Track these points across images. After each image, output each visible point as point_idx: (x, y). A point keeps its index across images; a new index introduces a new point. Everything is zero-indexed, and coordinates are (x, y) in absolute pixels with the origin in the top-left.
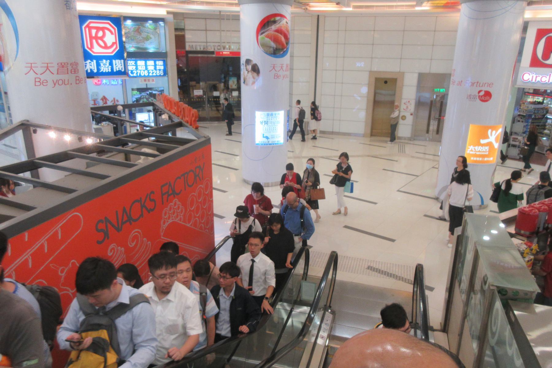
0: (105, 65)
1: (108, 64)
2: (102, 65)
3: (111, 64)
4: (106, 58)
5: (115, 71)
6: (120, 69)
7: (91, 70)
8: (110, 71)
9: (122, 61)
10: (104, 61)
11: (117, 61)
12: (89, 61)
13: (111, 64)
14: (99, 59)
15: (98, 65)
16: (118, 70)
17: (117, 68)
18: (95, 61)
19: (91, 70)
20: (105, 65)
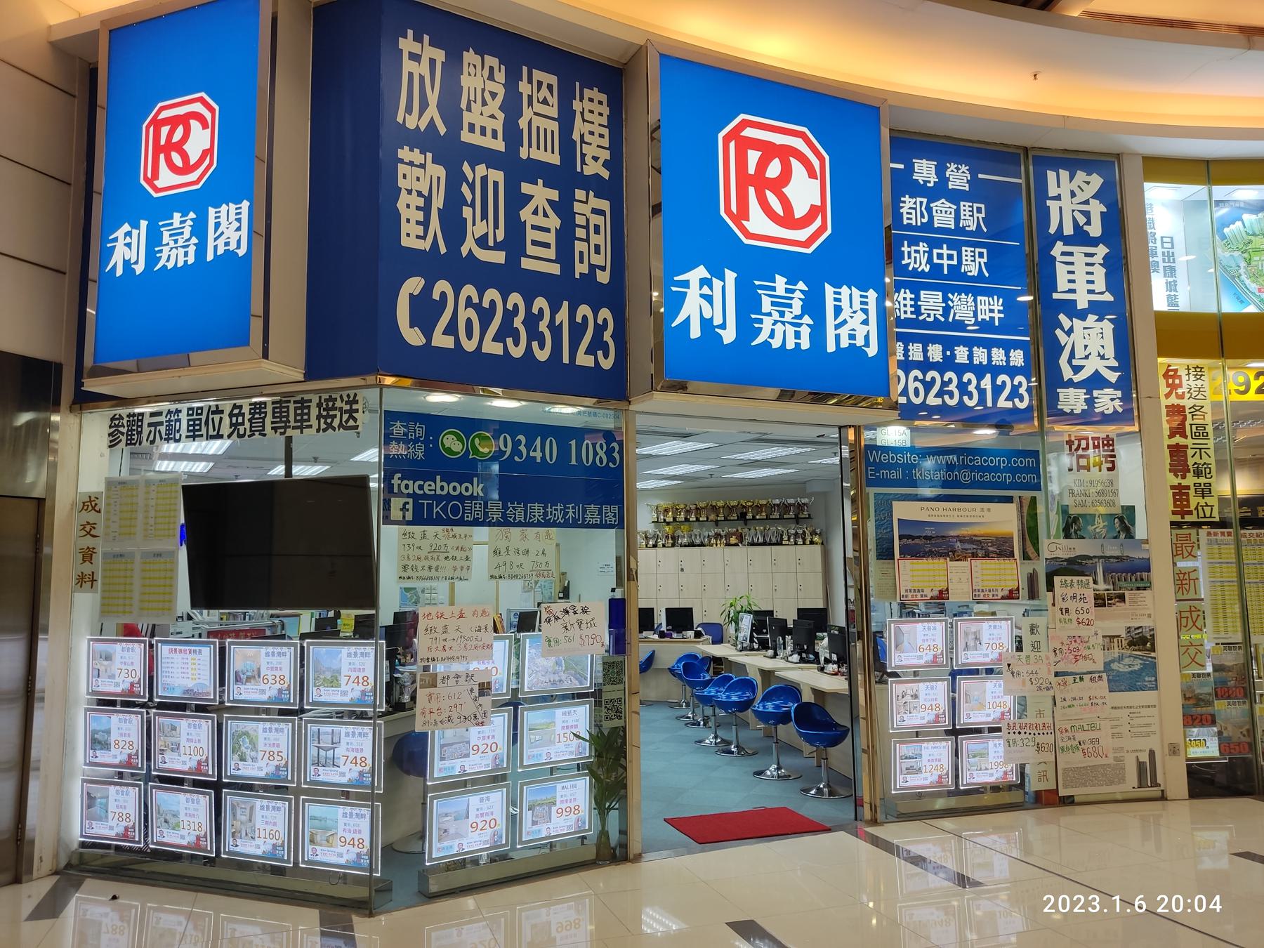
0: (782, 305)
1: (797, 310)
2: (766, 304)
3: (814, 305)
4: (793, 266)
5: (831, 348)
6: (860, 342)
7: (706, 323)
8: (805, 344)
9: (872, 295)
10: (780, 283)
11: (845, 290)
12: (701, 272)
13: (814, 305)
14: (755, 266)
15: (748, 304)
16: (845, 343)
17: (844, 332)
18: (730, 276)
19: (706, 323)
20: (782, 305)
